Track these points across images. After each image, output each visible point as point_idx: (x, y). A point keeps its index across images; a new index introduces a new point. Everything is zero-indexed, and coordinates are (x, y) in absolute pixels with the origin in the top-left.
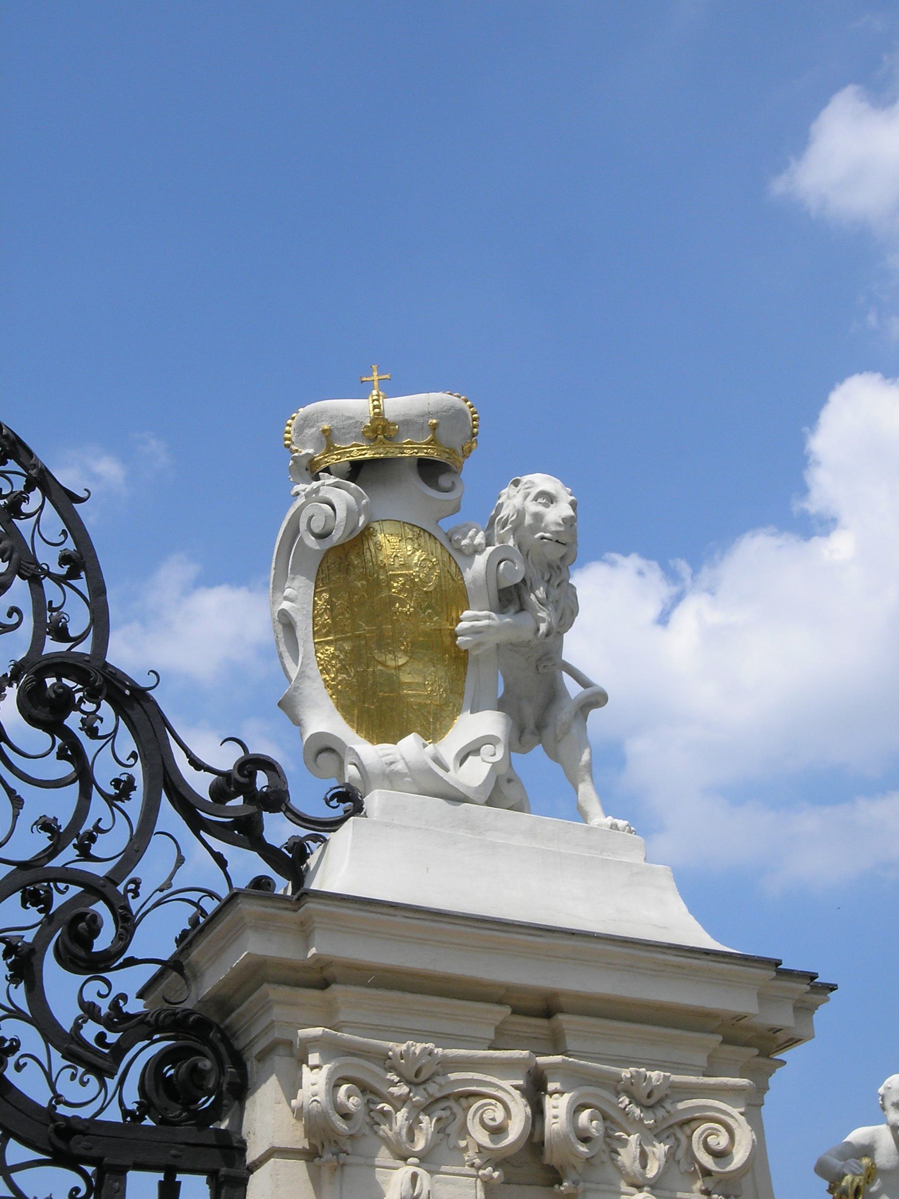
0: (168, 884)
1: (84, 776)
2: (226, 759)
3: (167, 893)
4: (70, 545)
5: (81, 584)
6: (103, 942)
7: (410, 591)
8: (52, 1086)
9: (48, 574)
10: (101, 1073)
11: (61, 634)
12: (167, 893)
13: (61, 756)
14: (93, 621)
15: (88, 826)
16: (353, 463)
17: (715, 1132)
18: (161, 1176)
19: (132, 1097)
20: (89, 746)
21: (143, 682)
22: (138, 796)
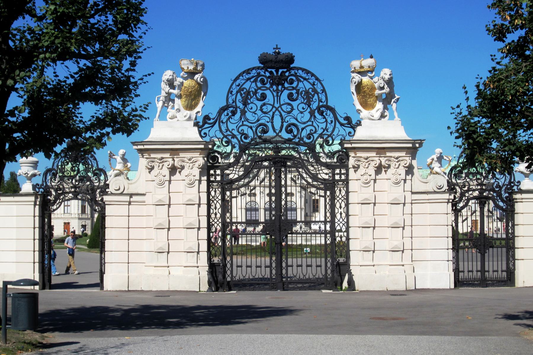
1: (326, 121)
2: (346, 115)
4: (322, 88)
5: (324, 94)
11: (322, 102)
19: (335, 160)
20: (327, 117)
22: (333, 122)
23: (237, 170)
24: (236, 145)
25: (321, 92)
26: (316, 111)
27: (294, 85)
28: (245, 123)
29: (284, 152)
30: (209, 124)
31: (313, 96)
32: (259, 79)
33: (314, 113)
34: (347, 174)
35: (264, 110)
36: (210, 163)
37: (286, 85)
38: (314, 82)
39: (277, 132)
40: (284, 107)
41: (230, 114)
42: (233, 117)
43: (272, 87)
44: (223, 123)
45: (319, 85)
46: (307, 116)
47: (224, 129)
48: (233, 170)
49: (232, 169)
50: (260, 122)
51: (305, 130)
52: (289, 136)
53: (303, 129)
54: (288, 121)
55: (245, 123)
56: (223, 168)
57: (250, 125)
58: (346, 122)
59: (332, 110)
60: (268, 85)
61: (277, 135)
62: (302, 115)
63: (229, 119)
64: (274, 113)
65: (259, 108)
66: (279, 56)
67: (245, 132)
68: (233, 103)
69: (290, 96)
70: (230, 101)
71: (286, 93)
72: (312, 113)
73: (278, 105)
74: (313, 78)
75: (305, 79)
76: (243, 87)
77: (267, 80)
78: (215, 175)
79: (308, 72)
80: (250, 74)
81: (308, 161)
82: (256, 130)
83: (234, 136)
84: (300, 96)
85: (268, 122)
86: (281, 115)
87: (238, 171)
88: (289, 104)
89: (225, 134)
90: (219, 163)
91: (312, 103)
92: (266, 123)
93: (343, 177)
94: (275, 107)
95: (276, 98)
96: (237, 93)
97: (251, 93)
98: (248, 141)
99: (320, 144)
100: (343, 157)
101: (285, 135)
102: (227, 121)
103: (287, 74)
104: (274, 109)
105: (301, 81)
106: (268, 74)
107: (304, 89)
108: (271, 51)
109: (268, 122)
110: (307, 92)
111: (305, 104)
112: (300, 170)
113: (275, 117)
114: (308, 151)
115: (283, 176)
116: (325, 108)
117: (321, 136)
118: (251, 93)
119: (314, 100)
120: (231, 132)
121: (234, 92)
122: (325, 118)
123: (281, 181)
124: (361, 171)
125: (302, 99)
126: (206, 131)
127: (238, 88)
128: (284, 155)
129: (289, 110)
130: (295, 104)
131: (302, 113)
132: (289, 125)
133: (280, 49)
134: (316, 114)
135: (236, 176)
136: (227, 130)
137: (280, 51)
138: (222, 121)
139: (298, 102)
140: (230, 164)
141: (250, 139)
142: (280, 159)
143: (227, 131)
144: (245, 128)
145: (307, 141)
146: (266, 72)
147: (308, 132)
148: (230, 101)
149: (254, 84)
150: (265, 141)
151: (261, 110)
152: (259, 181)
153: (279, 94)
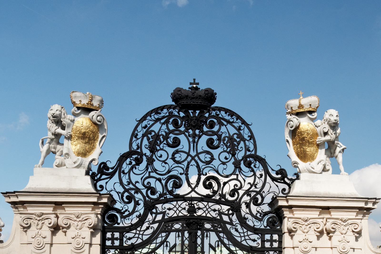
0: (269, 191)
1: (255, 174)
2: (278, 168)
3: (269, 192)
4: (250, 134)
5: (252, 141)
6: (259, 201)
7: (308, 135)
8: (253, 223)
9: (246, 140)
10: (260, 221)
11: (249, 151)
12: (269, 192)
13: (251, 171)
14: (254, 147)
15: (256, 183)
19: (265, 224)
21: (263, 157)
23: (141, 233)
24: (140, 202)
25: (248, 139)
26: (242, 162)
27: (216, 129)
28: (152, 174)
29: (200, 213)
30: (106, 174)
31: (239, 143)
32: (171, 120)
33: (240, 164)
34: (280, 242)
35: (176, 159)
36: (106, 223)
37: (205, 129)
38: (240, 127)
39: (193, 186)
40: (202, 156)
41: (134, 163)
42: (137, 167)
43: (187, 130)
44: (124, 173)
45: (246, 130)
46: (231, 167)
47: (125, 180)
48: (136, 233)
49: (134, 231)
50: (171, 174)
51: (227, 185)
52: (208, 192)
53: (225, 184)
54: (206, 174)
55: (152, 174)
56: (123, 231)
57: (158, 176)
58: (279, 176)
59: (263, 161)
60: (182, 129)
61: (193, 190)
62: (225, 166)
63: (131, 169)
64: (189, 163)
65: (170, 156)
66: (197, 92)
67: (153, 185)
68: (138, 149)
69: (210, 143)
70: (135, 147)
71: (204, 138)
72: (237, 165)
73: (195, 153)
74: (239, 121)
75: (228, 122)
76: (151, 129)
77: (182, 123)
78: (113, 239)
79: (232, 114)
80: (160, 114)
81: (231, 223)
82: (166, 183)
83: (138, 191)
84: (222, 143)
85: (181, 174)
86: (198, 166)
87: (143, 235)
88: (208, 153)
89: (127, 187)
90: (119, 224)
91: (237, 152)
92: (179, 175)
93: (276, 245)
94: (191, 156)
95: (192, 145)
96: (143, 136)
97: (161, 137)
98: (155, 197)
99: (246, 203)
100: (275, 219)
101: (202, 191)
102: (129, 172)
103: (207, 115)
104: (189, 158)
105: (223, 124)
106: (182, 114)
107: (227, 135)
108: (186, 86)
109: (181, 174)
110: (231, 139)
111: (228, 153)
112: (221, 235)
113: (191, 167)
114: (231, 212)
115: (199, 241)
116: (253, 160)
117: (248, 193)
118: (161, 137)
119: (239, 148)
120: (134, 185)
121: (140, 135)
122: (253, 171)
123: (196, 248)
124: (299, 236)
125: (225, 147)
126: (102, 183)
127: (145, 130)
128: (200, 216)
129: (208, 159)
130: (215, 153)
131: (224, 163)
132: (208, 178)
133: (198, 84)
134: (242, 166)
135: (140, 241)
136: (130, 182)
137: (199, 86)
138: (123, 171)
139: (220, 150)
140: (132, 225)
141: (158, 194)
142: (196, 221)
143: (129, 184)
144: (152, 181)
145: (230, 199)
146: (180, 113)
147: (232, 188)
148: (135, 147)
149: (164, 127)
150: (178, 198)
151: (173, 158)
152: (168, 248)
153: (196, 140)
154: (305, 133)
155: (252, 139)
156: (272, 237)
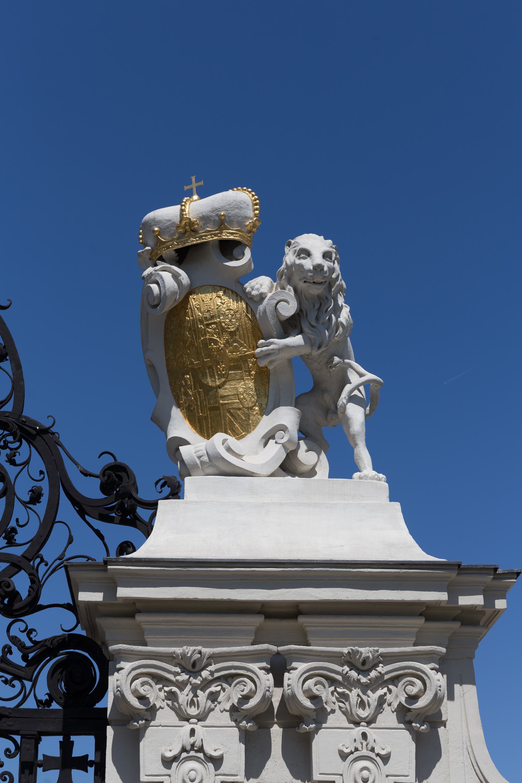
15: (13, 524)
16: (176, 251)
17: (412, 684)
18: (60, 738)
19: (42, 690)
21: (47, 424)
22: (45, 499)
154: (208, 325)
155: (8, 358)
156: (66, 746)
